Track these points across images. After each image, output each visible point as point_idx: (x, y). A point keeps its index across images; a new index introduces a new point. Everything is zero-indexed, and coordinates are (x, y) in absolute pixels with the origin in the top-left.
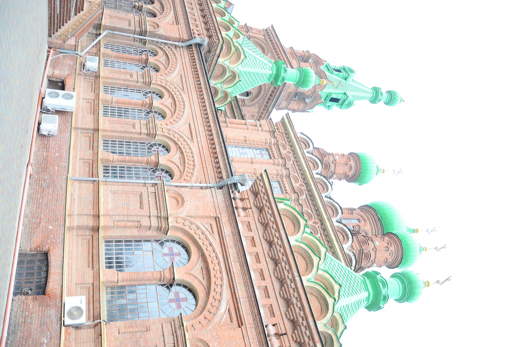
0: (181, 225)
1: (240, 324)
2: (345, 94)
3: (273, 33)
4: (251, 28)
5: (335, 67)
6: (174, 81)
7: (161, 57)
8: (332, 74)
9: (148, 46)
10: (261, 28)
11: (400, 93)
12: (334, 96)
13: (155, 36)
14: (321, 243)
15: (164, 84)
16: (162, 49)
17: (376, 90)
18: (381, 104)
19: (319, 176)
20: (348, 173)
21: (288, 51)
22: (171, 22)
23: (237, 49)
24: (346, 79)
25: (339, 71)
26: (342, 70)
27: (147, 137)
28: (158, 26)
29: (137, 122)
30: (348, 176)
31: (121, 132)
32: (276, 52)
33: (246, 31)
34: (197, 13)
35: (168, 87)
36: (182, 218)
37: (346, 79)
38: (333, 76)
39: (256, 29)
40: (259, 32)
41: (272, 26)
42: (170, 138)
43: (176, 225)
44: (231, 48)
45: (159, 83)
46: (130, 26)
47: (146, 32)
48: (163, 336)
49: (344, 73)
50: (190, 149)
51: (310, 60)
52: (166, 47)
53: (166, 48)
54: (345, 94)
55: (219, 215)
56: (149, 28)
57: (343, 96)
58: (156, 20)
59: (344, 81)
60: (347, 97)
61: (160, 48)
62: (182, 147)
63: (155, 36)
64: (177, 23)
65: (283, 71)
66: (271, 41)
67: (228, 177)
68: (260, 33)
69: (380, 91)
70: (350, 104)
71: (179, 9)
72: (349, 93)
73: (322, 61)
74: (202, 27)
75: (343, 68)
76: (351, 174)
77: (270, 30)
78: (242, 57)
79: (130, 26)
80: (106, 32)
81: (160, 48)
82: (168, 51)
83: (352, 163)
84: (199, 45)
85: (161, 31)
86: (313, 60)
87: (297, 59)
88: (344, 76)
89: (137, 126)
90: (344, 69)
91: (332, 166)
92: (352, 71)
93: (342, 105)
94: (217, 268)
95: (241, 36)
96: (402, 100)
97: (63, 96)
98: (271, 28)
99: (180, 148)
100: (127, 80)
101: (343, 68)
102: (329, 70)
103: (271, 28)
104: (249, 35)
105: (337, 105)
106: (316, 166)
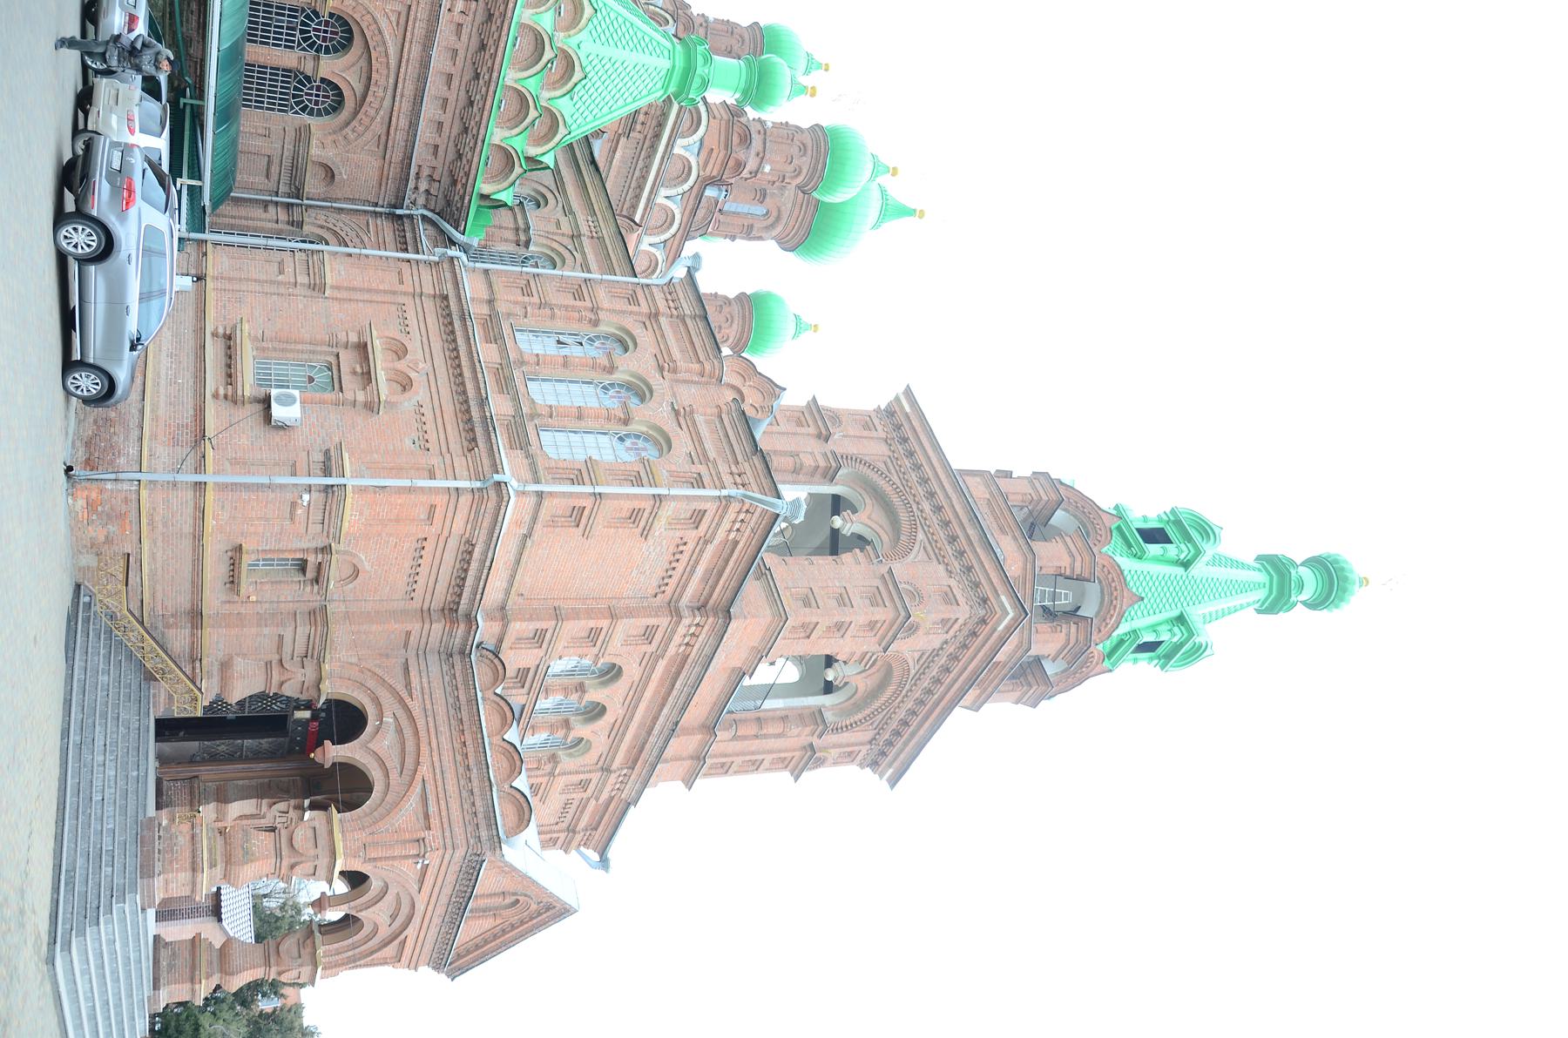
2: (1181, 619)
3: (916, 423)
4: (836, 417)
5: (1145, 519)
8: (1140, 558)
10: (869, 406)
11: (1357, 562)
12: (1149, 637)
17: (1277, 566)
18: (1298, 617)
21: (978, 490)
24: (1186, 565)
25: (1154, 536)
26: (1171, 532)
32: (946, 524)
33: (819, 436)
37: (1186, 565)
39: (853, 414)
40: (866, 427)
41: (908, 392)
49: (1183, 546)
51: (1059, 517)
54: (1181, 619)
57: (1176, 629)
59: (1180, 570)
60: (1191, 634)
66: (918, 467)
68: (874, 434)
69: (1293, 572)
70: (1198, 652)
72: (1195, 614)
73: (1100, 512)
75: (1172, 518)
77: (995, 629)
86: (1082, 522)
87: (1017, 534)
88: (1182, 557)
90: (1178, 523)
92: (1206, 531)
93: (1168, 657)
96: (1365, 582)
98: (907, 408)
101: (1172, 518)
102: (1129, 546)
103: (907, 408)
104: (834, 453)
105: (1151, 659)
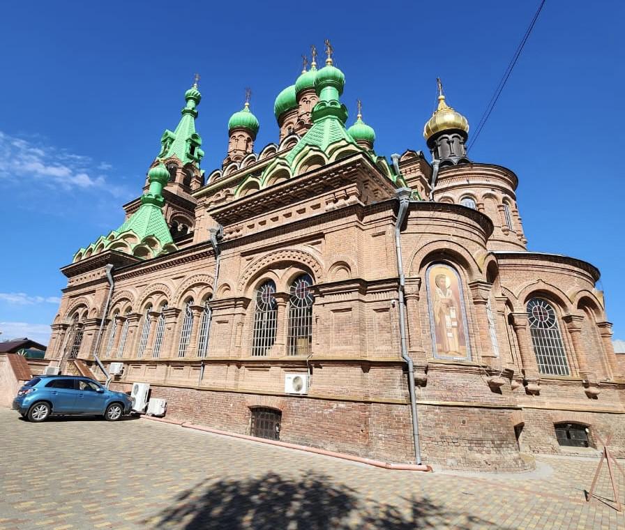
0: (244, 287)
1: (321, 235)
2: (187, 141)
6: (139, 293)
7: (122, 306)
9: (111, 316)
13: (102, 311)
14: (273, 162)
15: (141, 303)
16: (114, 305)
19: (242, 164)
20: (246, 139)
22: (94, 297)
23: (124, 237)
27: (179, 317)
28: (94, 309)
29: (166, 326)
30: (248, 138)
34: (88, 274)
35: (143, 299)
36: (238, 285)
38: (169, 153)
42: (182, 296)
43: (243, 290)
44: (120, 243)
45: (139, 307)
46: (91, 335)
47: (97, 320)
48: (323, 304)
50: (190, 278)
52: (113, 300)
53: (114, 301)
54: (187, 141)
55: (239, 253)
56: (95, 316)
58: (89, 311)
61: (113, 306)
62: (188, 286)
63: (102, 311)
64: (94, 291)
65: (150, 197)
67: (212, 246)
71: (82, 291)
74: (100, 270)
76: (247, 136)
78: (131, 232)
79: (91, 335)
80: (95, 355)
81: (113, 306)
82: (116, 299)
83: (237, 134)
84: (113, 272)
85: (99, 307)
89: (170, 326)
91: (238, 153)
94: (278, 255)
95: (112, 234)
97: (136, 393)
99: (190, 287)
100: (134, 336)
106: (235, 167)
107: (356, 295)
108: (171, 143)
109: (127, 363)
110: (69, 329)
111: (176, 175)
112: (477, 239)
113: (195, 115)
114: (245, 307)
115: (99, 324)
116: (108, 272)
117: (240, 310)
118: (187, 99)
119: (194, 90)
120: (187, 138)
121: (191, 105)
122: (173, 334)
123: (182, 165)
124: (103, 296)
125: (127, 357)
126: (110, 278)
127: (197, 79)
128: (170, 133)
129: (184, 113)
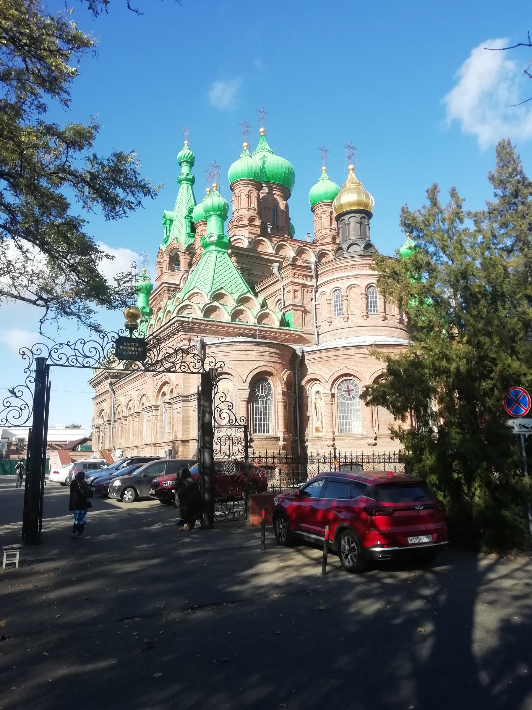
2: (185, 218)
13: (111, 414)
31: (138, 433)
37: (172, 221)
38: (170, 237)
47: (108, 421)
54: (185, 218)
63: (111, 414)
84: (111, 384)
107: (181, 404)
108: (171, 225)
109: (124, 449)
110: (101, 428)
111: (179, 261)
112: (254, 358)
113: (192, 181)
114: (157, 410)
115: (110, 424)
116: (108, 386)
117: (154, 413)
118: (180, 164)
119: (185, 152)
120: (184, 216)
121: (185, 169)
122: (139, 429)
123: (183, 249)
124: (110, 403)
125: (124, 445)
126: (110, 390)
127: (186, 134)
128: (169, 214)
129: (180, 182)
